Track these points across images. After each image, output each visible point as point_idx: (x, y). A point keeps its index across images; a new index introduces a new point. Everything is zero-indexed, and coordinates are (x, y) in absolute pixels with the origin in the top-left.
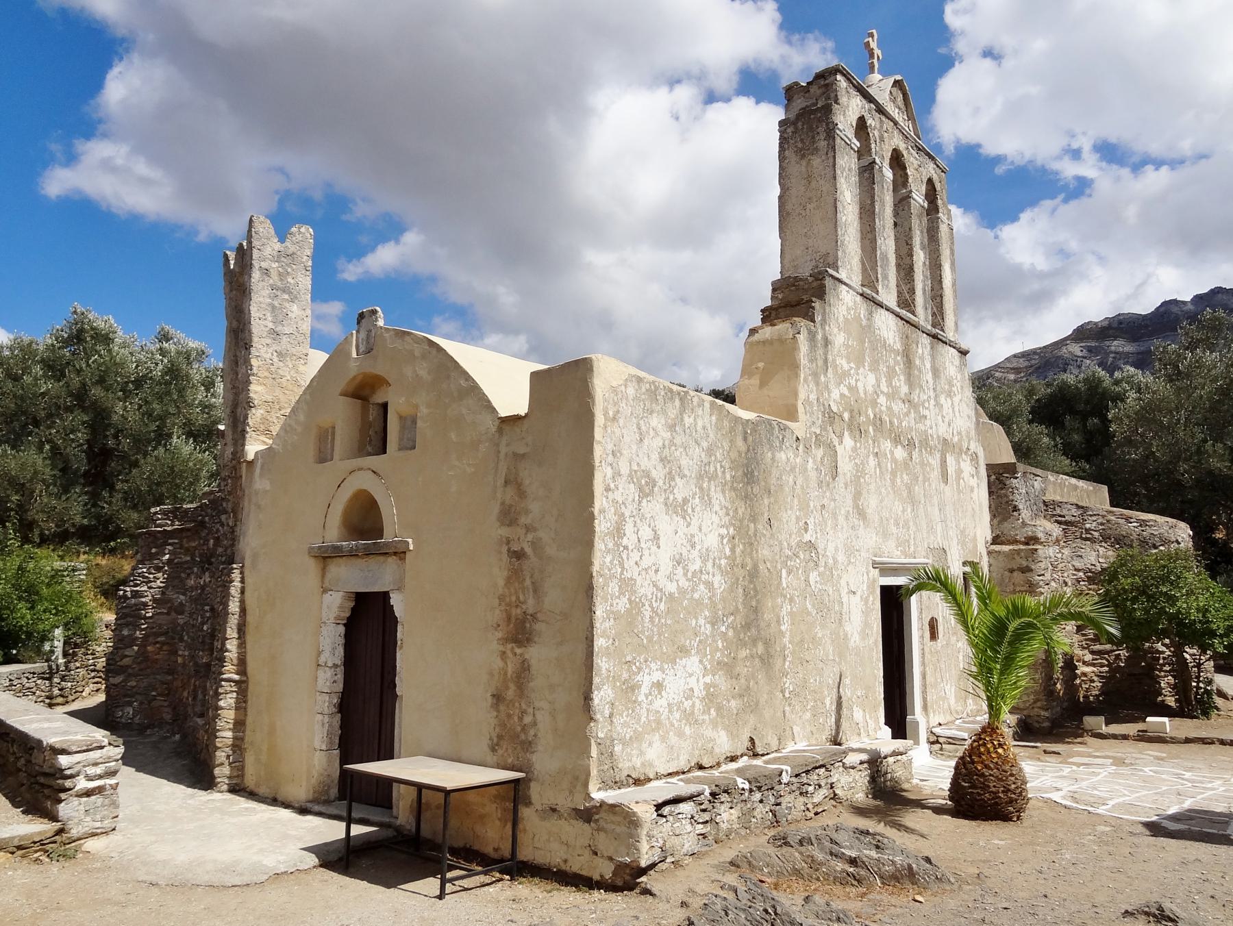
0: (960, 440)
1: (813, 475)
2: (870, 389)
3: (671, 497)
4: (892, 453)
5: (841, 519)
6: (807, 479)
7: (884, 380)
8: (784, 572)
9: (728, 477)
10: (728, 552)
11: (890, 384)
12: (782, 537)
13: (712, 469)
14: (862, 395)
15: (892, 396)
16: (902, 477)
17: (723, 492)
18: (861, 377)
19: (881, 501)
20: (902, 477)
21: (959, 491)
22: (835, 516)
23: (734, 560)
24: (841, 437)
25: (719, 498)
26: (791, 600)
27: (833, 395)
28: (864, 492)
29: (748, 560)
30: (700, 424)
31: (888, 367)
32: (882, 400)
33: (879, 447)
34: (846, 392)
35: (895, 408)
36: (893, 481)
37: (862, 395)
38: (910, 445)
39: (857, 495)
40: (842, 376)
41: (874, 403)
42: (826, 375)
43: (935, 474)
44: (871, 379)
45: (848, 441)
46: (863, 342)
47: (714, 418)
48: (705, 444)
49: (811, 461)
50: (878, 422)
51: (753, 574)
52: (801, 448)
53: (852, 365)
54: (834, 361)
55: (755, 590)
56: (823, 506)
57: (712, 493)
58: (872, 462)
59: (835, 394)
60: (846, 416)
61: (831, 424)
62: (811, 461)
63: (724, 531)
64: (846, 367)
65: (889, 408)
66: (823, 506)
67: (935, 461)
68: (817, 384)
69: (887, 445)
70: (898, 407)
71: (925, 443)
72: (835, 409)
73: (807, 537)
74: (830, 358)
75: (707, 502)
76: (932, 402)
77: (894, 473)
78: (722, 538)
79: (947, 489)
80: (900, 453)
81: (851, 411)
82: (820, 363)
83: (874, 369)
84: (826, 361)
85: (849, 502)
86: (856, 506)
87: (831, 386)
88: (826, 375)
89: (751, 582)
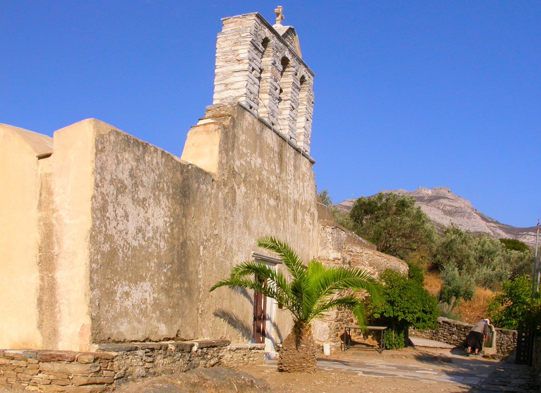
0: (306, 204)
1: (221, 201)
2: (258, 165)
3: (136, 196)
4: (268, 201)
5: (236, 227)
6: (217, 202)
7: (266, 163)
8: (201, 248)
9: (171, 191)
10: (169, 230)
11: (269, 165)
12: (202, 229)
13: (161, 186)
14: (253, 167)
15: (272, 172)
16: (272, 214)
17: (168, 199)
18: (253, 158)
19: (260, 223)
20: (272, 214)
21: (303, 230)
22: (232, 224)
23: (173, 235)
24: (239, 185)
25: (164, 201)
26: (205, 263)
27: (236, 163)
28: (250, 216)
29: (181, 238)
30: (155, 161)
31: (270, 158)
32: (265, 173)
33: (261, 195)
34: (244, 164)
35: (271, 178)
36: (267, 215)
37: (253, 167)
38: (277, 198)
39: (246, 218)
40: (241, 156)
41: (260, 174)
42: (233, 152)
43: (291, 218)
44: (259, 161)
45: (243, 189)
46: (256, 142)
47: (163, 159)
48: (157, 172)
49: (220, 193)
50: (261, 183)
51: (184, 245)
52: (215, 186)
53: (249, 151)
54: (238, 147)
55: (184, 253)
56: (226, 218)
57: (161, 198)
58: (256, 202)
59: (238, 163)
60: (243, 175)
61: (234, 177)
62: (220, 193)
63: (167, 219)
64: (245, 151)
65: (268, 178)
66: (226, 218)
67: (291, 211)
68: (227, 155)
69: (265, 196)
70: (273, 179)
71: (286, 200)
72: (237, 170)
73: (216, 232)
74: (236, 145)
75: (158, 202)
76: (292, 181)
77: (268, 211)
78: (166, 222)
79: (296, 226)
80: (272, 202)
81: (246, 174)
82: (230, 146)
83: (261, 156)
84: (233, 146)
85: (241, 219)
86: (245, 222)
87: (236, 158)
88: (233, 152)
89: (182, 249)
